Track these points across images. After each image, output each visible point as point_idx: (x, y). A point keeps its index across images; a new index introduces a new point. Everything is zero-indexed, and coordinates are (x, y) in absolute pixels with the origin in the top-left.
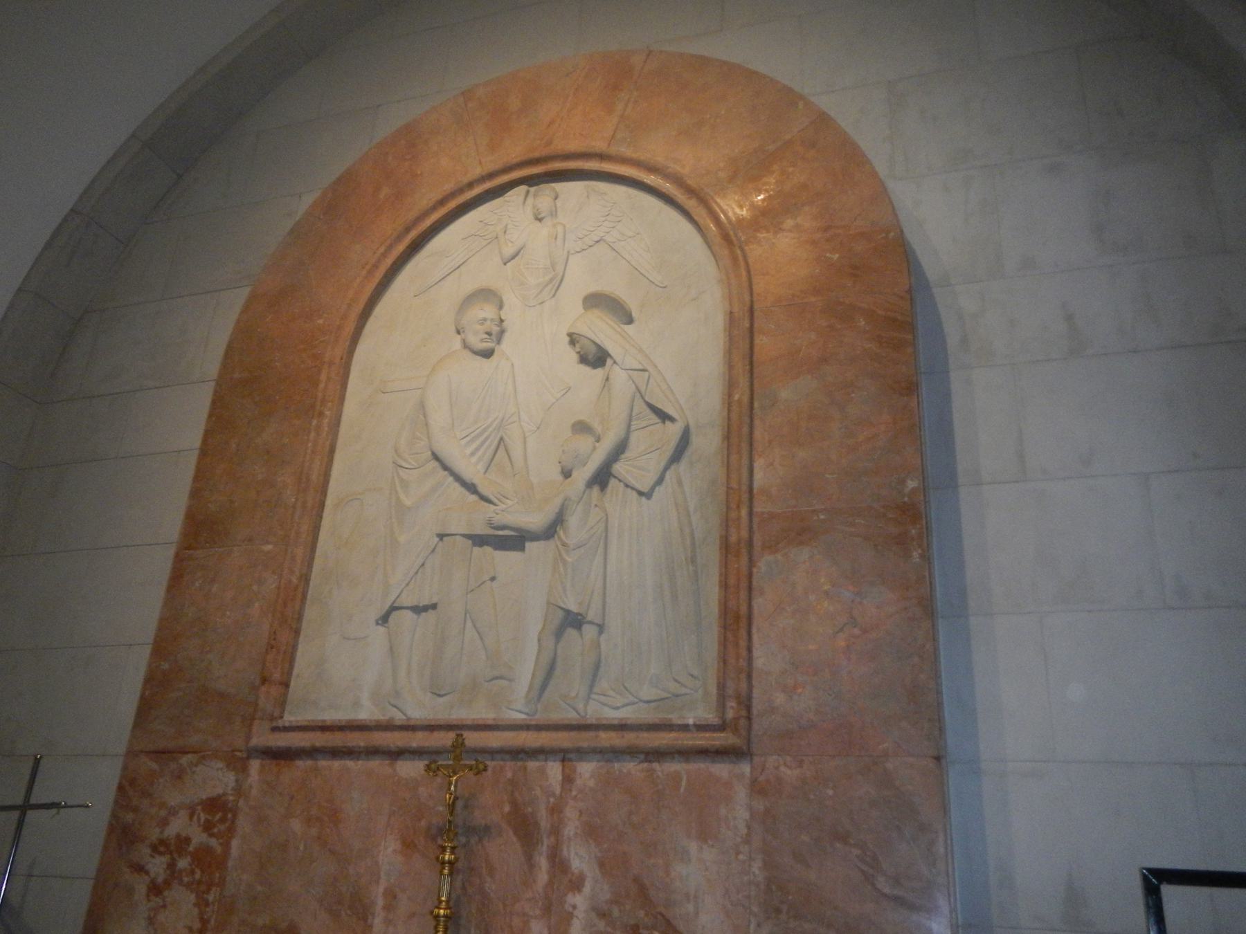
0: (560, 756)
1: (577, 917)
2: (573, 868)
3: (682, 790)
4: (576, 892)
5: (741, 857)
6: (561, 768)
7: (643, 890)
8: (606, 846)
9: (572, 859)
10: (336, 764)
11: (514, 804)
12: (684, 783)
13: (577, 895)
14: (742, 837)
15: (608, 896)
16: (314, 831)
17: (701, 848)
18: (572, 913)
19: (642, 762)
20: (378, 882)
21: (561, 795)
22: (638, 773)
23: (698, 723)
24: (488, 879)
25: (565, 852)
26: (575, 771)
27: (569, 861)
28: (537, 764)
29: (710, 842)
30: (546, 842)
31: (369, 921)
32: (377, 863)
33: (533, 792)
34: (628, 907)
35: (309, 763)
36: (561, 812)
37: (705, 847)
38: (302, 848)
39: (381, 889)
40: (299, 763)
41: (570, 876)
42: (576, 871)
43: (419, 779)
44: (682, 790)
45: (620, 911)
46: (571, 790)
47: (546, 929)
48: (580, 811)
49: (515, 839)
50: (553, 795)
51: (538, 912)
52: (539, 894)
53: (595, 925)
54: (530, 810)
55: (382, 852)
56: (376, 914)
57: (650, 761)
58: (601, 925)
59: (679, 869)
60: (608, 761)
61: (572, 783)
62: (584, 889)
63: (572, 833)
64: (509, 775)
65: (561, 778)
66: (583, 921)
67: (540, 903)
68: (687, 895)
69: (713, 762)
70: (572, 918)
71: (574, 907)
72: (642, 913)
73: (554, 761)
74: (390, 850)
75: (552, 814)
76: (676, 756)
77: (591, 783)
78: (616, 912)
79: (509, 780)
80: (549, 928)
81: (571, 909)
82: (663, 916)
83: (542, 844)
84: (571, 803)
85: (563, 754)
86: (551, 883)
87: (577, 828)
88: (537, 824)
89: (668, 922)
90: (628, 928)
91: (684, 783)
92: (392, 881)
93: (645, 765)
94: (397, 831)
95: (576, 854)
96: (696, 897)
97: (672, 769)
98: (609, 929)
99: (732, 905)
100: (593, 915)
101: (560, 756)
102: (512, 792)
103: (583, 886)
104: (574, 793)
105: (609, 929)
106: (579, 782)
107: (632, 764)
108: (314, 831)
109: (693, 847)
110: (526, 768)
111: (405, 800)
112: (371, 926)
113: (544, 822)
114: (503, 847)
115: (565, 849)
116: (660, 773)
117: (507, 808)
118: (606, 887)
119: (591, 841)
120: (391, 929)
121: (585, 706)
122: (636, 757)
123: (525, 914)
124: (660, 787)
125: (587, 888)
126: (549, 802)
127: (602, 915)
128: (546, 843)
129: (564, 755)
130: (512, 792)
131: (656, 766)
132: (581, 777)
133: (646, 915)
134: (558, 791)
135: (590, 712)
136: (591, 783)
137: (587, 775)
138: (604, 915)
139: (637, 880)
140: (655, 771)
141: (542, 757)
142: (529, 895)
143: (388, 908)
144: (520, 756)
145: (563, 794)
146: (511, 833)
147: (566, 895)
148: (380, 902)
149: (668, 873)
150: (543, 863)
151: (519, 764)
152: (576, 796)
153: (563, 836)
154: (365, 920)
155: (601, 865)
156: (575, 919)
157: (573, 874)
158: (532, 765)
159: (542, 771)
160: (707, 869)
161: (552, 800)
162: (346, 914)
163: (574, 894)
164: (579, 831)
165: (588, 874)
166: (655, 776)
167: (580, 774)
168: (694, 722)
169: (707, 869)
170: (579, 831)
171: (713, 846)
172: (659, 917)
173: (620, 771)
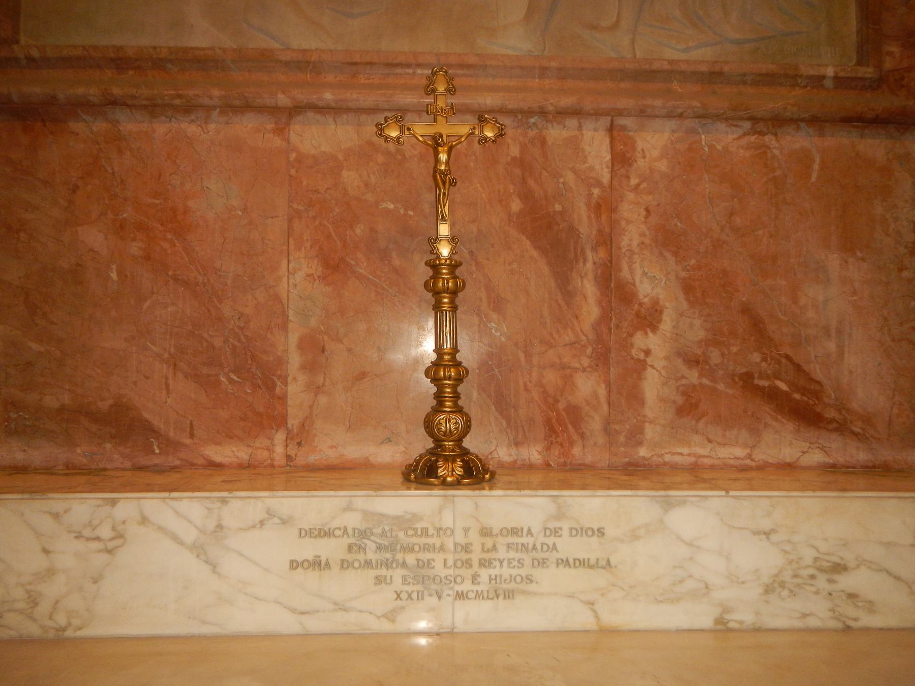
0: (605, 121)
1: (652, 367)
2: (641, 296)
3: (813, 179)
4: (648, 330)
5: (905, 274)
6: (607, 141)
7: (757, 326)
8: (693, 262)
9: (638, 283)
10: (161, 128)
11: (526, 196)
12: (816, 167)
13: (650, 334)
14: (906, 247)
15: (701, 334)
16: (135, 248)
17: (846, 262)
18: (645, 361)
19: (745, 134)
20: (284, 328)
21: (611, 186)
22: (742, 151)
23: (842, 74)
24: (494, 316)
25: (625, 273)
26: (634, 148)
27: (634, 285)
28: (565, 134)
29: (859, 254)
30: (590, 255)
31: (278, 390)
32: (277, 298)
33: (561, 180)
34: (734, 349)
35: (100, 126)
36: (613, 210)
37: (851, 260)
38: (114, 276)
39: (294, 338)
40: (76, 126)
41: (636, 307)
42: (646, 300)
43: (340, 157)
44: (813, 179)
45: (723, 355)
46: (628, 178)
47: (603, 386)
48: (647, 210)
49: (535, 253)
50: (599, 184)
51: (586, 362)
52: (586, 336)
53: (683, 377)
54: (558, 207)
55: (285, 279)
56: (290, 379)
57: (761, 133)
58: (693, 376)
59: (812, 292)
60: (692, 131)
61: (630, 165)
62: (662, 326)
63: (635, 243)
64: (515, 151)
65: (609, 157)
66: (663, 372)
67: (589, 351)
68: (827, 331)
69: (862, 136)
70: (645, 369)
71: (647, 352)
72: (756, 357)
73: (595, 130)
74: (299, 276)
75: (599, 217)
76: (803, 125)
77: (663, 166)
78: (715, 356)
79: (514, 159)
80: (608, 384)
81: (642, 356)
82: (787, 357)
83: (585, 260)
84: (631, 196)
85: (610, 118)
86: (605, 317)
87: (642, 235)
88: (572, 230)
89: (798, 368)
90: (737, 379)
91: (816, 167)
92: (313, 322)
93: (753, 138)
94: (308, 245)
95: (645, 274)
96: (839, 332)
97: (797, 146)
98: (705, 381)
99: (893, 340)
100: (679, 362)
101: (605, 121)
102: (524, 178)
103: (660, 321)
104: (634, 181)
105: (705, 381)
106: (641, 163)
107: (731, 137)
108: (135, 248)
109: (833, 261)
110: (543, 142)
111: (317, 191)
112: (283, 398)
113: (585, 225)
114: (515, 266)
115: (625, 266)
116: (776, 152)
117: (516, 205)
118: (698, 322)
119: (668, 255)
120: (323, 400)
121: (633, 42)
122: (736, 126)
123: (563, 367)
124: (778, 173)
125: (666, 325)
126: (590, 195)
127: (693, 362)
128: (592, 259)
129: (612, 120)
130: (524, 178)
131: (769, 139)
132: (644, 157)
133: (764, 359)
134: (606, 177)
135: (639, 54)
136: (663, 166)
137: (656, 153)
138: (698, 362)
139: (746, 310)
140: (769, 148)
141: (572, 122)
142: (568, 337)
143: (310, 367)
144: (532, 120)
145: (615, 183)
146: (527, 243)
147: (631, 335)
148: (295, 360)
149: (795, 300)
150: (590, 289)
151: (532, 133)
152: (638, 186)
153: (620, 248)
154: (271, 387)
155: (688, 288)
156: (649, 370)
157: (641, 304)
158: (555, 133)
159: (574, 144)
160: (855, 293)
161: (596, 191)
162: (231, 381)
163: (646, 334)
164: (647, 241)
165: (667, 304)
166: (769, 155)
167: (643, 150)
168: (836, 73)
169: (855, 293)
170: (647, 241)
171: (863, 260)
172: (783, 361)
173: (711, 147)
